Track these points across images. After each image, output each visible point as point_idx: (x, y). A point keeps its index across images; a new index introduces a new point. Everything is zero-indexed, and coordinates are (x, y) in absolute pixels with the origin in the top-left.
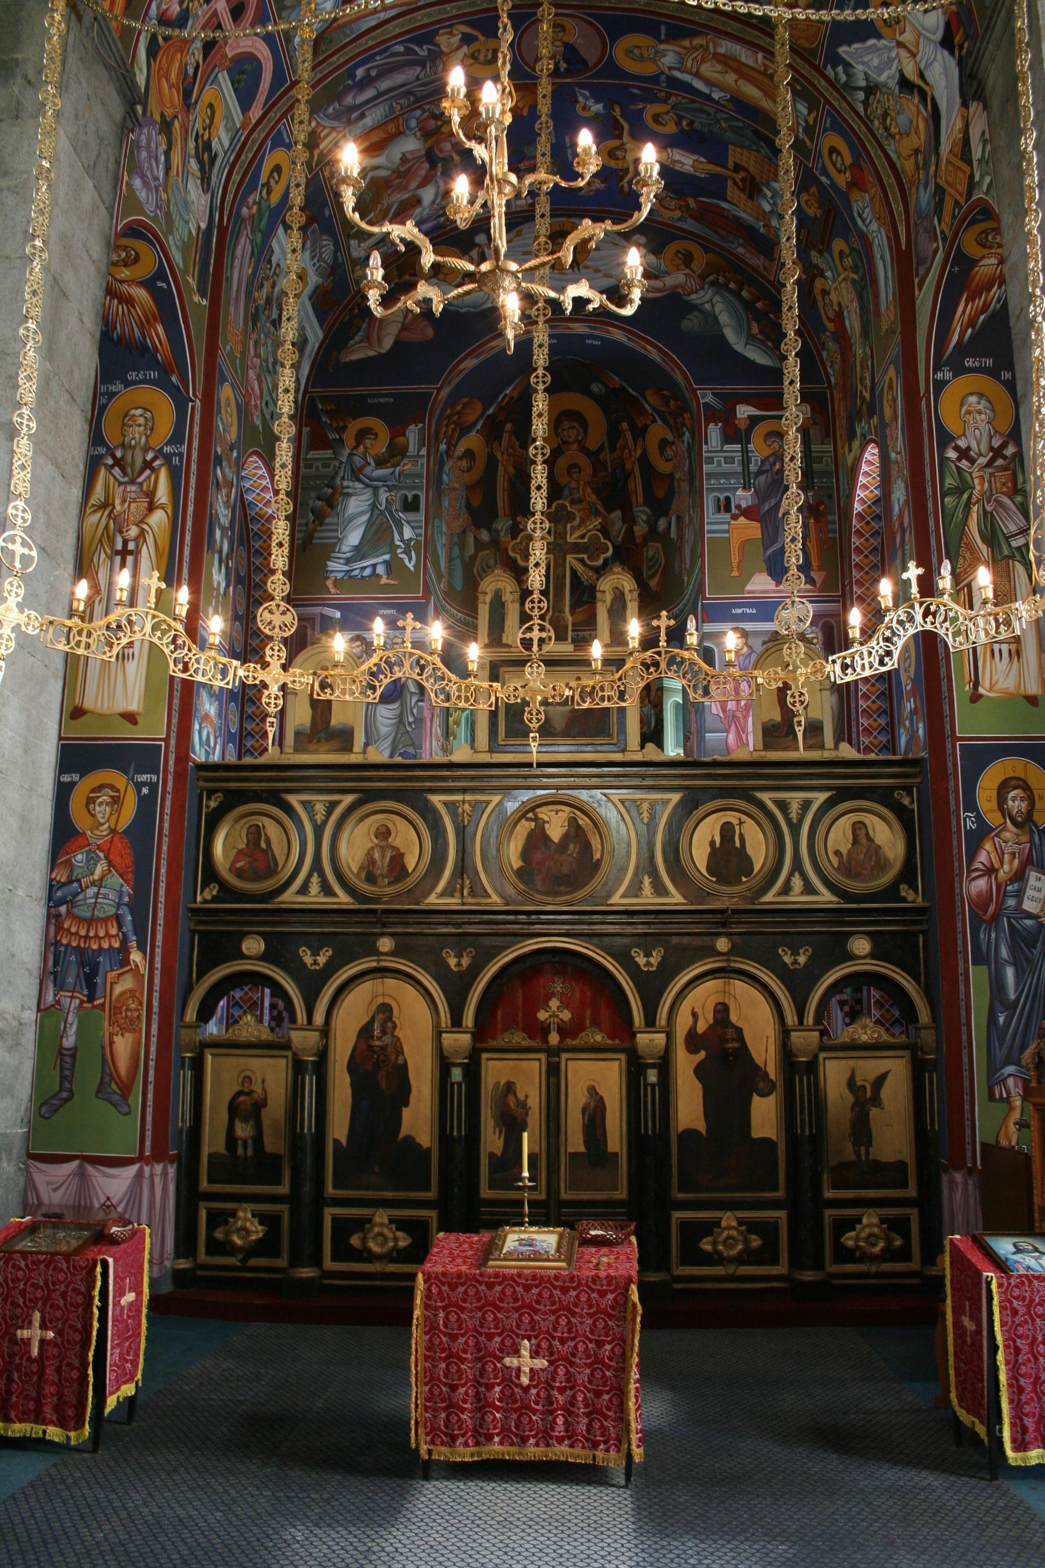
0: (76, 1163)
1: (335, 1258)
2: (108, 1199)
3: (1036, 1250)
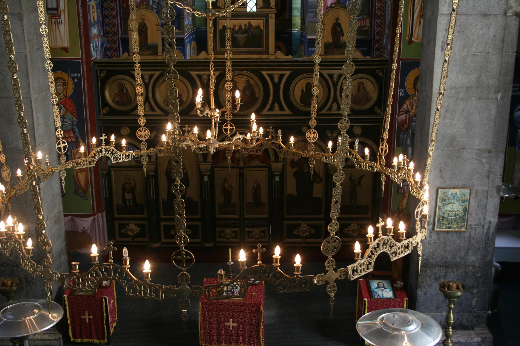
0: (70, 217)
1: (165, 238)
2: (84, 228)
3: (384, 287)
